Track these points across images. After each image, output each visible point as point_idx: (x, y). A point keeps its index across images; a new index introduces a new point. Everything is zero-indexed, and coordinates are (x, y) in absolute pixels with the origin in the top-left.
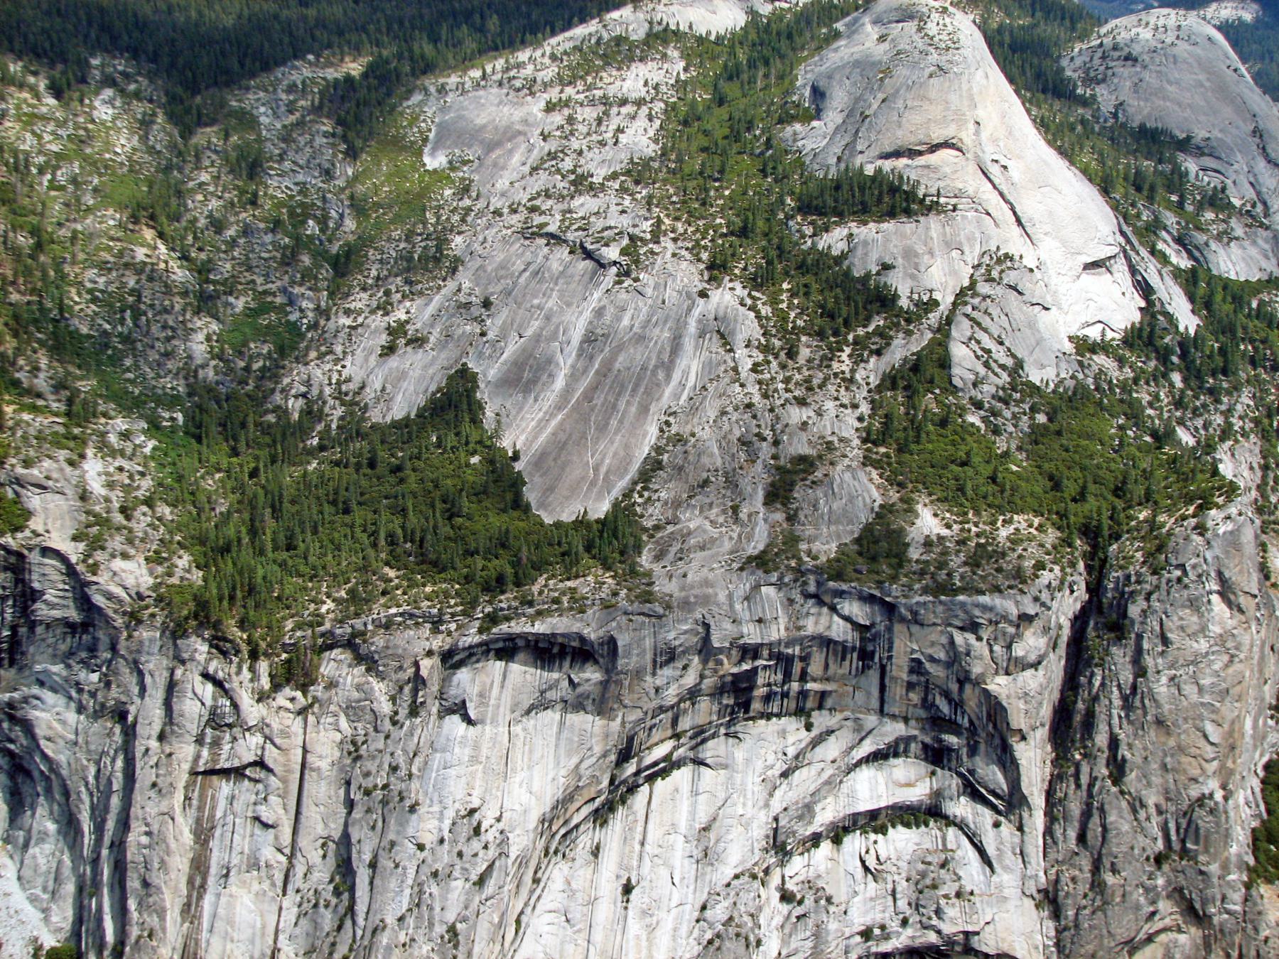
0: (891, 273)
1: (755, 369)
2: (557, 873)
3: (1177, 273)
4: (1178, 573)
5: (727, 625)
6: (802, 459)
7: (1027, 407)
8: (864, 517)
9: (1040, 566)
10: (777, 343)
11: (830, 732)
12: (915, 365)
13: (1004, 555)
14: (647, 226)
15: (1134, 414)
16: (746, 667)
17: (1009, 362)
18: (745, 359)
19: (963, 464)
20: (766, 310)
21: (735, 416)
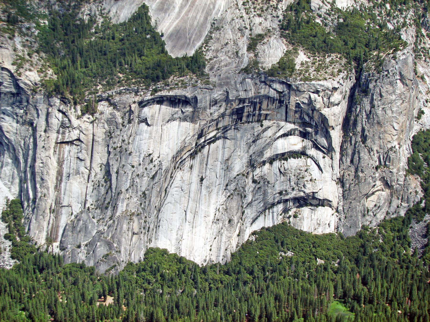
2: (179, 175)
4: (386, 73)
5: (234, 92)
7: (336, 16)
9: (340, 71)
11: (269, 127)
13: (328, 67)
15: (373, 19)
16: (241, 106)
19: (315, 37)
21: (237, 21)
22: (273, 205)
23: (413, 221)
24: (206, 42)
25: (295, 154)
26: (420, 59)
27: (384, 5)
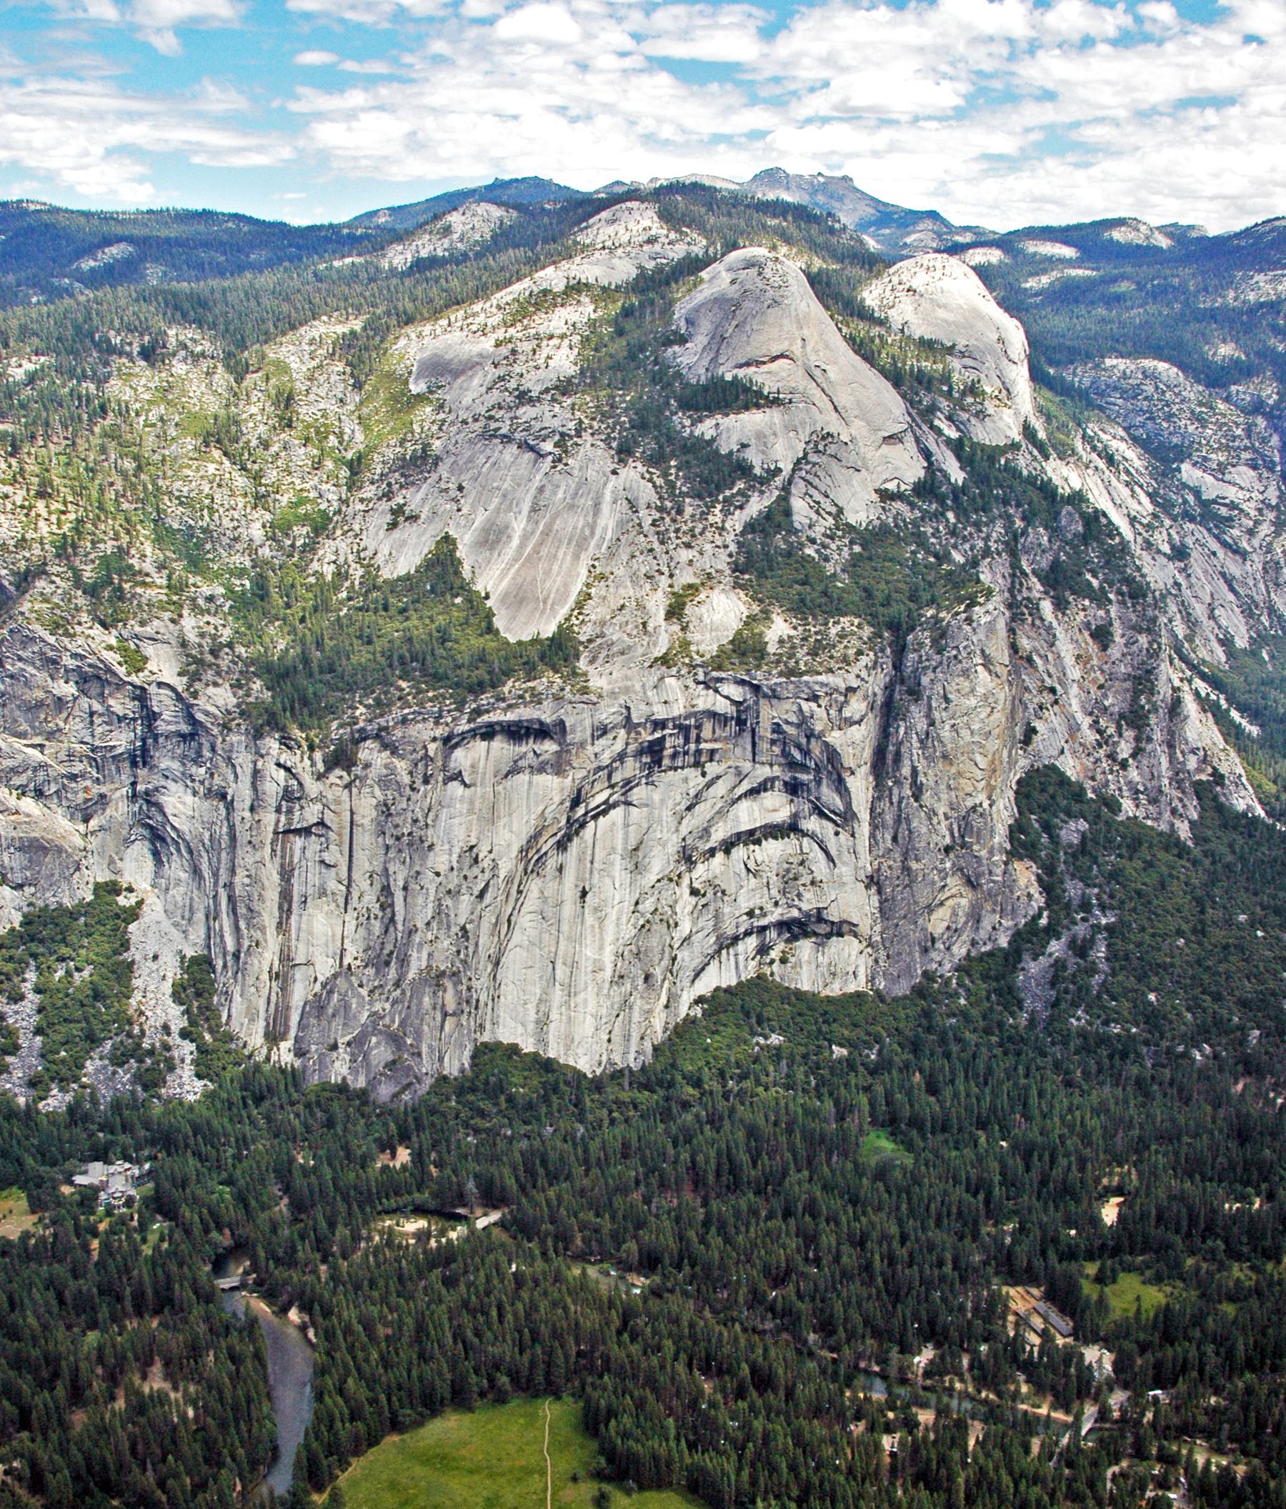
1: (654, 524)
5: (643, 707)
6: (690, 586)
8: (735, 625)
9: (860, 653)
10: (668, 504)
11: (718, 777)
12: (768, 516)
13: (834, 646)
14: (572, 425)
16: (658, 735)
18: (646, 517)
20: (659, 481)
21: (641, 558)
22: (736, 939)
23: (1026, 957)
24: (580, 605)
26: (1023, 621)
27: (943, 514)
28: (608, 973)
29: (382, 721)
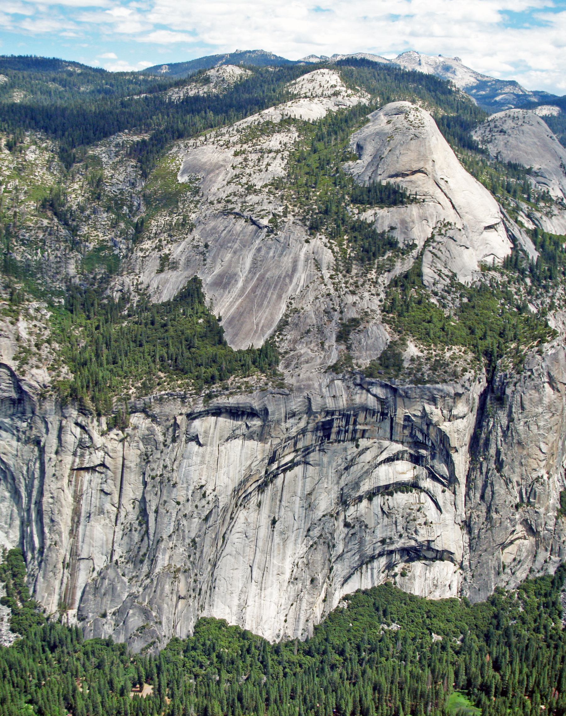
0: (395, 231)
1: (331, 277)
2: (242, 515)
3: (528, 231)
5: (319, 399)
6: (354, 320)
7: (458, 295)
8: (383, 347)
9: (465, 370)
11: (367, 449)
12: (406, 276)
13: (448, 365)
14: (281, 209)
15: (508, 298)
16: (328, 418)
17: (450, 274)
19: (429, 322)
20: (336, 249)
21: (322, 300)
25: (403, 487)
27: (523, 280)
28: (287, 576)
29: (147, 399)
